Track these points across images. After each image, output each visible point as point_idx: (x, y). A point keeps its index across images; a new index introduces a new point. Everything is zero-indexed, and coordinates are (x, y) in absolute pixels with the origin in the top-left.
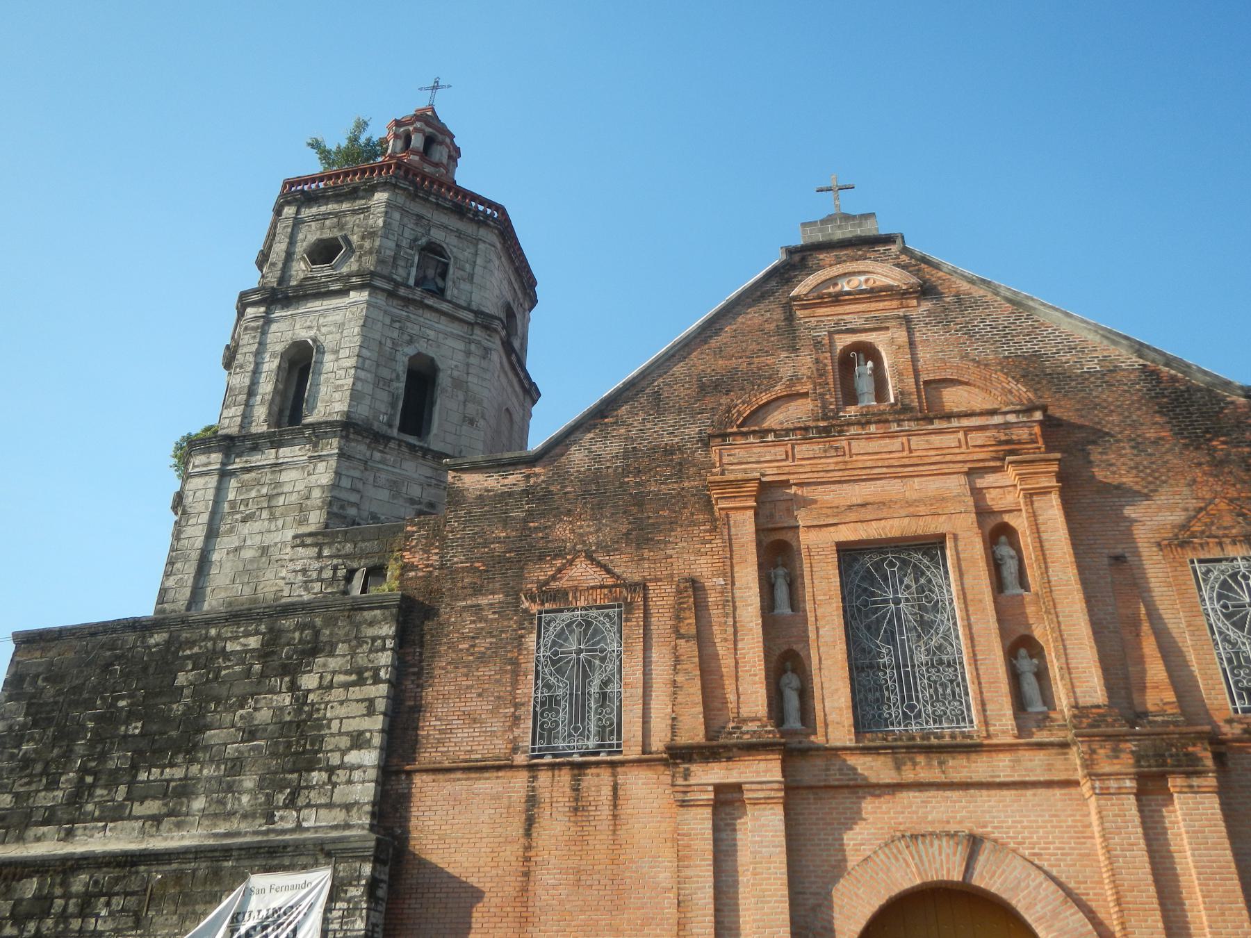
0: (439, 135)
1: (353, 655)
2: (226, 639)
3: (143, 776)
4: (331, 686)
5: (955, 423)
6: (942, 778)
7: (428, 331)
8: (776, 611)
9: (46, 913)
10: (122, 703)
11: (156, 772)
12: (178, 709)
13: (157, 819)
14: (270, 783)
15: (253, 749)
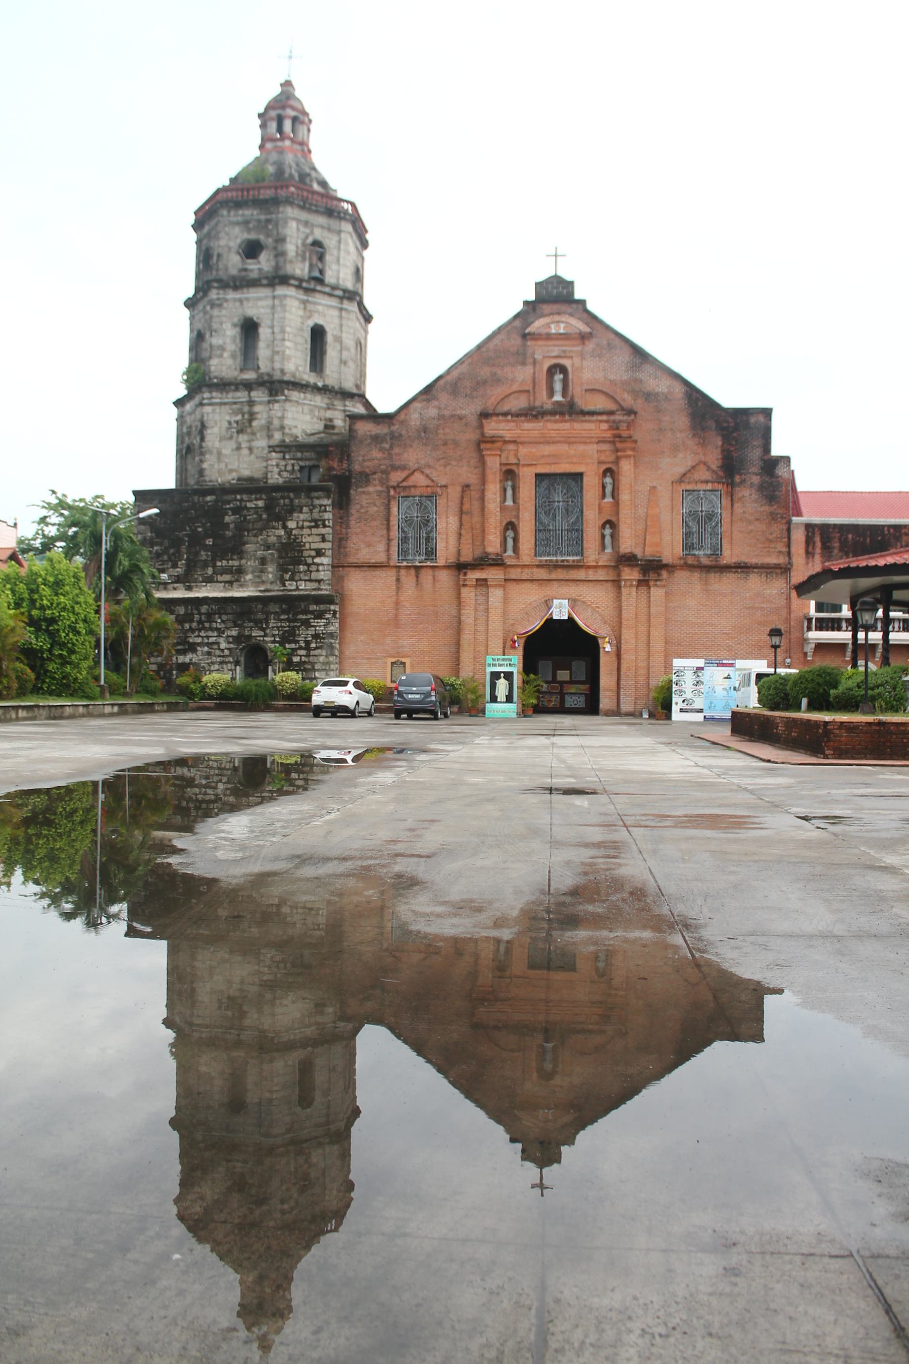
0: (301, 117)
1: (311, 511)
2: (246, 501)
3: (219, 564)
4: (302, 528)
5: (595, 418)
6: (567, 578)
7: (320, 308)
8: (507, 503)
9: (192, 621)
10: (200, 529)
11: (225, 563)
12: (229, 533)
13: (230, 583)
14: (282, 569)
15: (272, 554)
